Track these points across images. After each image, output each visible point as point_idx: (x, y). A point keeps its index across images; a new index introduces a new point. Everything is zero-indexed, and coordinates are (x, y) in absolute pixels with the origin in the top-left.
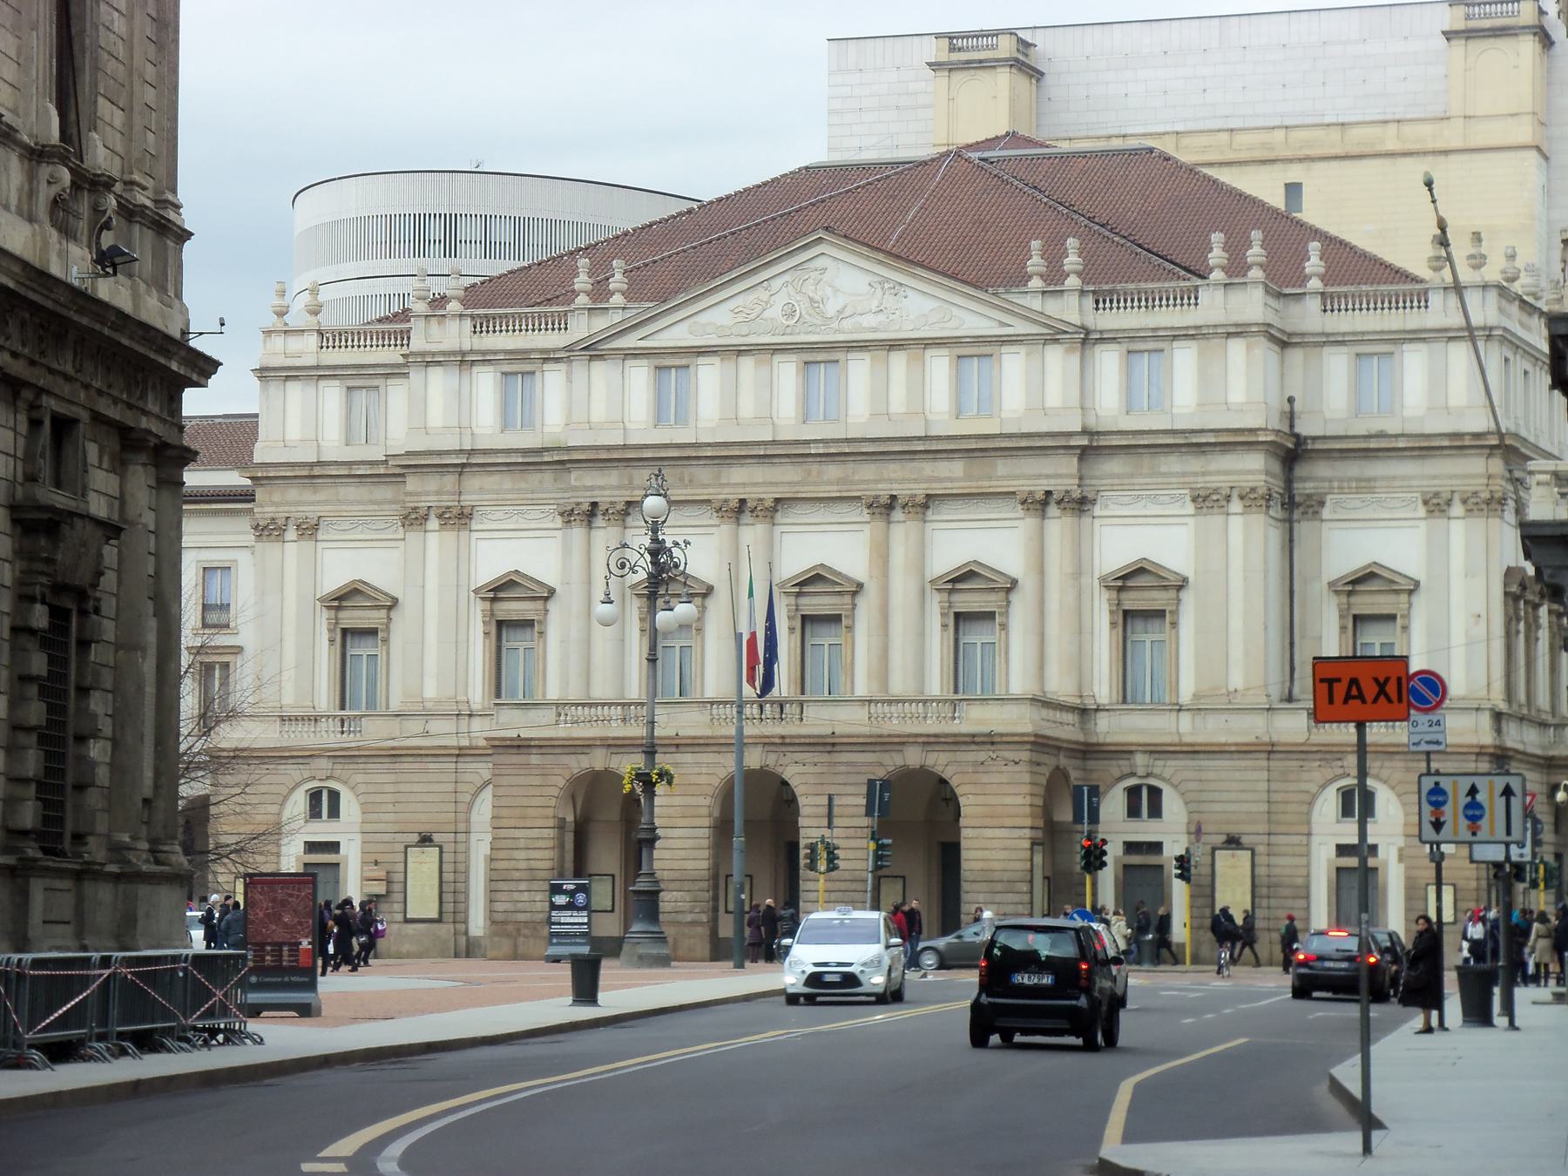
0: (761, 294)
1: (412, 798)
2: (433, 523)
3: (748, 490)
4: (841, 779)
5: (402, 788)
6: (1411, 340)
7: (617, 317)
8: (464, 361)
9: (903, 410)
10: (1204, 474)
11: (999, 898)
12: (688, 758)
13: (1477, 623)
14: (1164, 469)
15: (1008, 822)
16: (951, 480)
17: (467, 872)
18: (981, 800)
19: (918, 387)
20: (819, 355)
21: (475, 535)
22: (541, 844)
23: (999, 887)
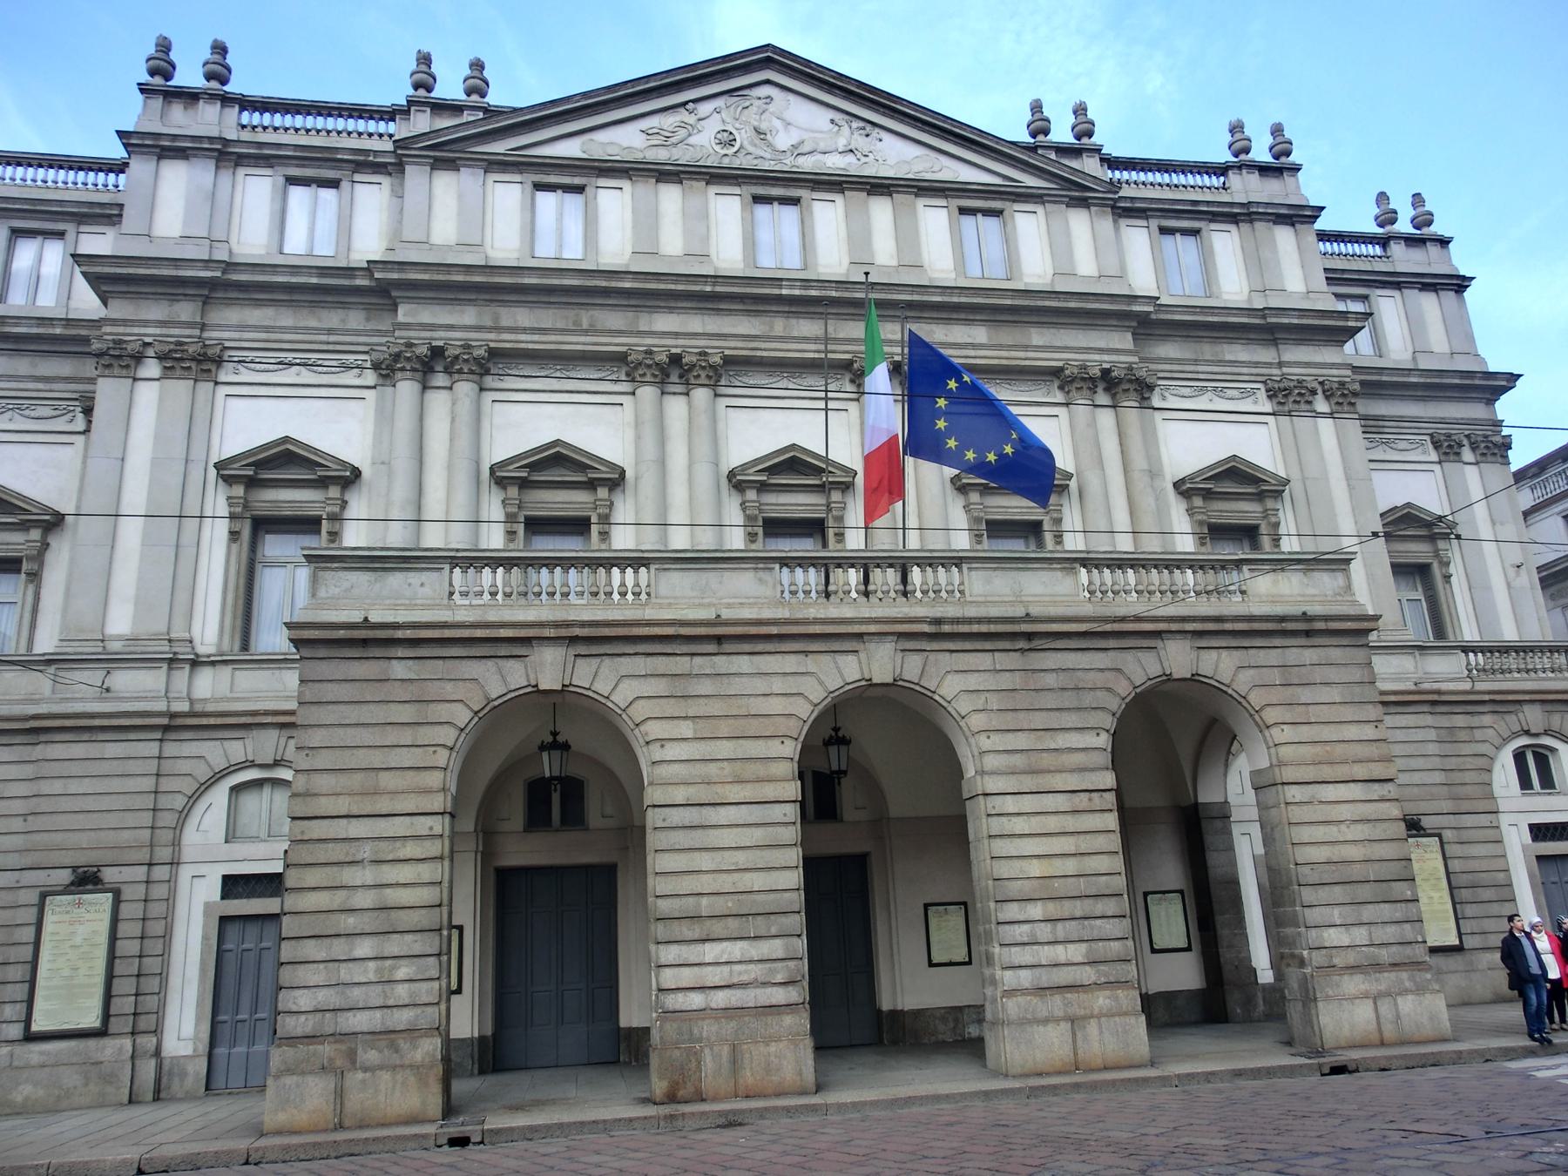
0: (682, 115)
1: (66, 804)
2: (151, 368)
3: (681, 342)
4: (1050, 701)
5: (46, 787)
6: (1384, 285)
7: (481, 115)
8: (226, 155)
9: (894, 263)
10: (1280, 365)
11: (1368, 913)
12: (743, 663)
13: (1518, 574)
14: (1229, 357)
15: (1360, 771)
16: (974, 346)
17: (167, 937)
18: (1305, 733)
19: (907, 236)
20: (777, 187)
21: (222, 391)
22: (410, 850)
23: (1364, 892)
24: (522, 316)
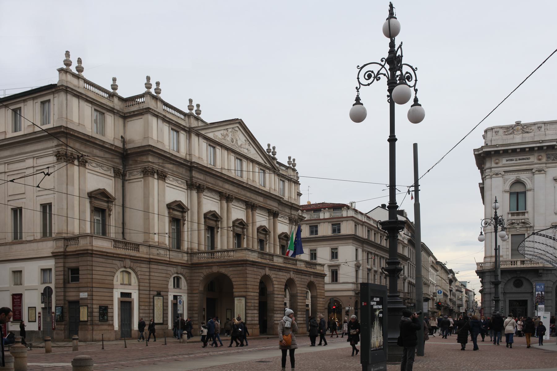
12: (281, 273)
20: (240, 156)
24: (209, 179)
